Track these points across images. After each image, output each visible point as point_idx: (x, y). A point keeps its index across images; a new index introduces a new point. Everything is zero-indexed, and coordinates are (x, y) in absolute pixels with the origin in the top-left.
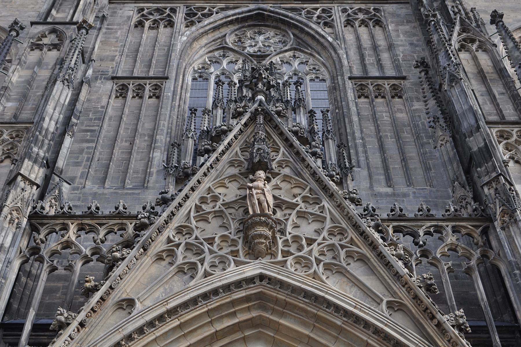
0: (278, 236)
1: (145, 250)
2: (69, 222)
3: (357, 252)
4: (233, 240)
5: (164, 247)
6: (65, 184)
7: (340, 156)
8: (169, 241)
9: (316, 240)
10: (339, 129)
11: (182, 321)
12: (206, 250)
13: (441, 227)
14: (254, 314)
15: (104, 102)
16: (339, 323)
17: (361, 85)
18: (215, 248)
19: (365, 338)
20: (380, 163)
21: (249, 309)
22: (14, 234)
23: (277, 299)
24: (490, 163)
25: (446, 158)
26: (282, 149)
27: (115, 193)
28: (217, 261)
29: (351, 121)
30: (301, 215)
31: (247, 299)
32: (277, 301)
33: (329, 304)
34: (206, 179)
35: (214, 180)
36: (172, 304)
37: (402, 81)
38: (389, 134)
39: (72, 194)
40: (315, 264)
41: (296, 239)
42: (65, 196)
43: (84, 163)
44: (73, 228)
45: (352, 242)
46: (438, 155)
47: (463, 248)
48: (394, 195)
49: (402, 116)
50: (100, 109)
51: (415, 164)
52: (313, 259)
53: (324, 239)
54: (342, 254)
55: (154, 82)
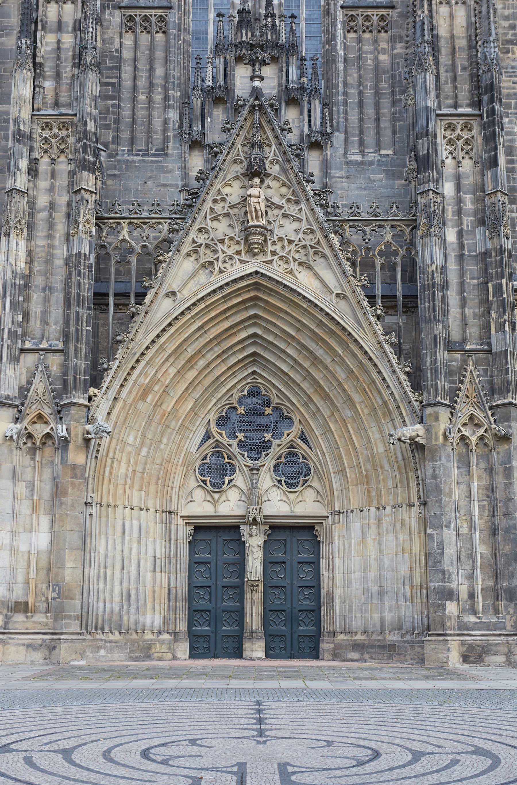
0: (268, 237)
1: (178, 251)
2: (122, 221)
3: (321, 252)
4: (237, 241)
5: (190, 248)
6: (102, 153)
7: (323, 124)
8: (194, 242)
9: (294, 241)
10: (327, 73)
11: (207, 304)
12: (220, 251)
13: (384, 226)
14: (252, 294)
15: (117, 46)
16: (305, 306)
17: (352, 15)
18: (225, 249)
19: (320, 318)
20: (356, 121)
21: (249, 291)
22: (90, 241)
23: (266, 286)
24: (427, 174)
25: (411, 122)
26: (274, 146)
27: (143, 160)
28: (227, 259)
29: (337, 69)
30: (285, 216)
31: (248, 286)
32: (266, 287)
33: (299, 294)
34: (217, 181)
35: (222, 181)
36: (200, 296)
37: (390, 11)
38: (369, 84)
39: (108, 161)
40: (292, 263)
41: (280, 239)
42: (104, 165)
43: (113, 125)
44: (125, 225)
45: (318, 243)
46: (405, 116)
47: (394, 246)
48: (362, 163)
49: (383, 57)
50: (114, 54)
51: (385, 124)
52: (291, 259)
53: (300, 241)
54: (311, 252)
55: (159, 12)
